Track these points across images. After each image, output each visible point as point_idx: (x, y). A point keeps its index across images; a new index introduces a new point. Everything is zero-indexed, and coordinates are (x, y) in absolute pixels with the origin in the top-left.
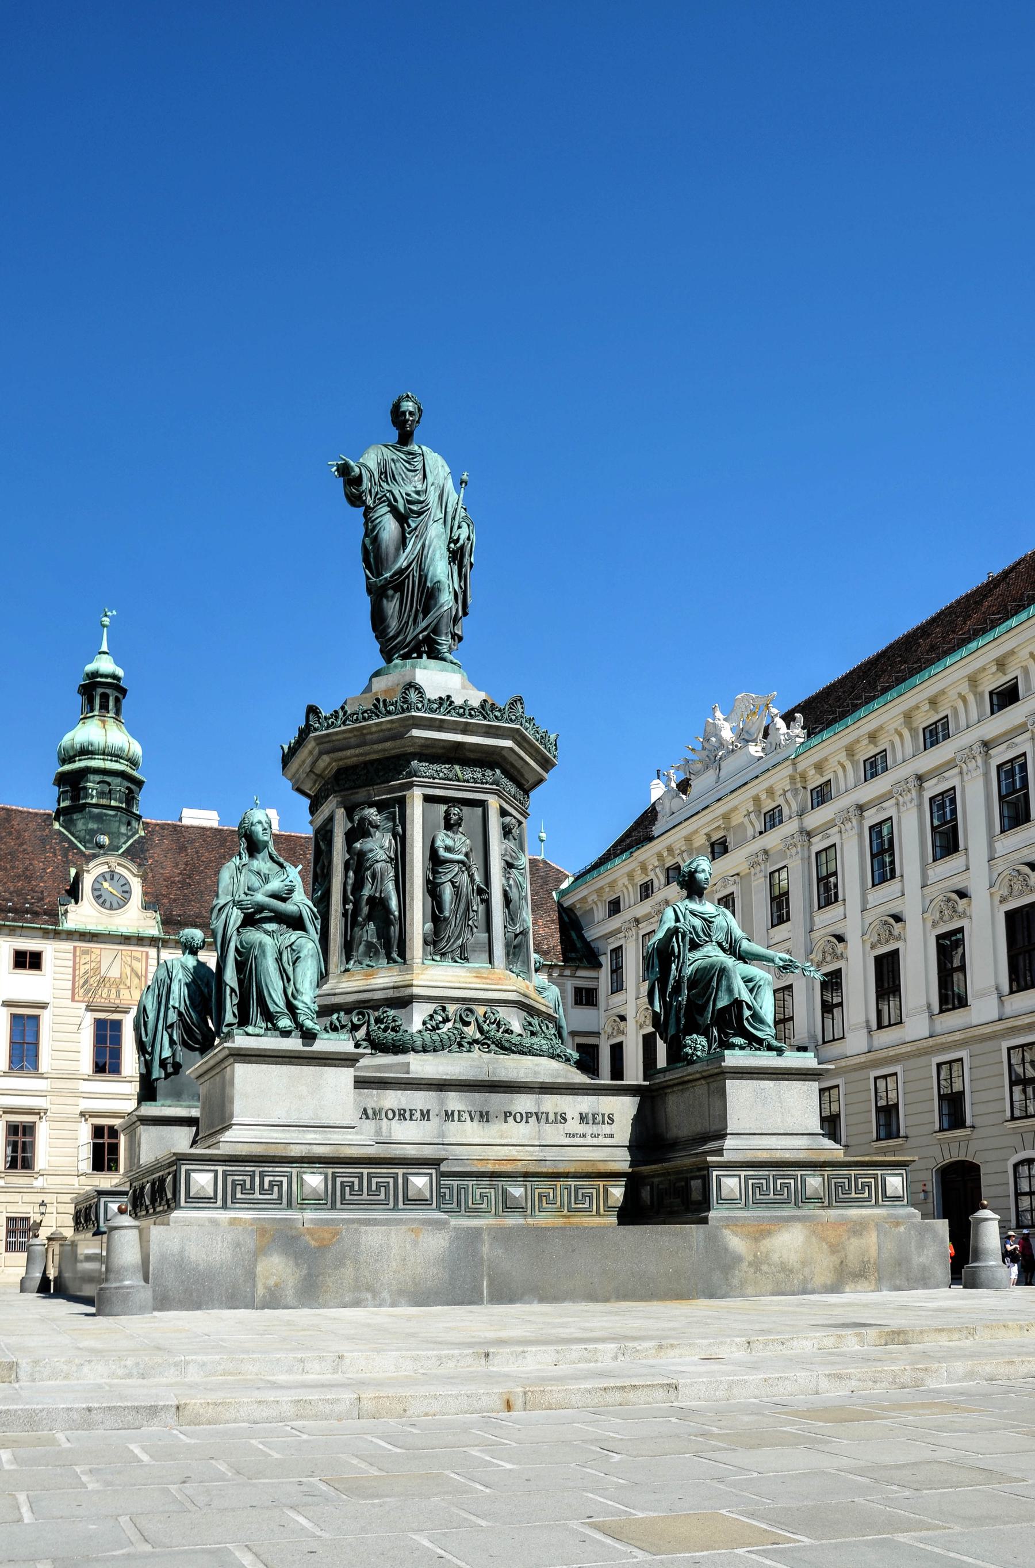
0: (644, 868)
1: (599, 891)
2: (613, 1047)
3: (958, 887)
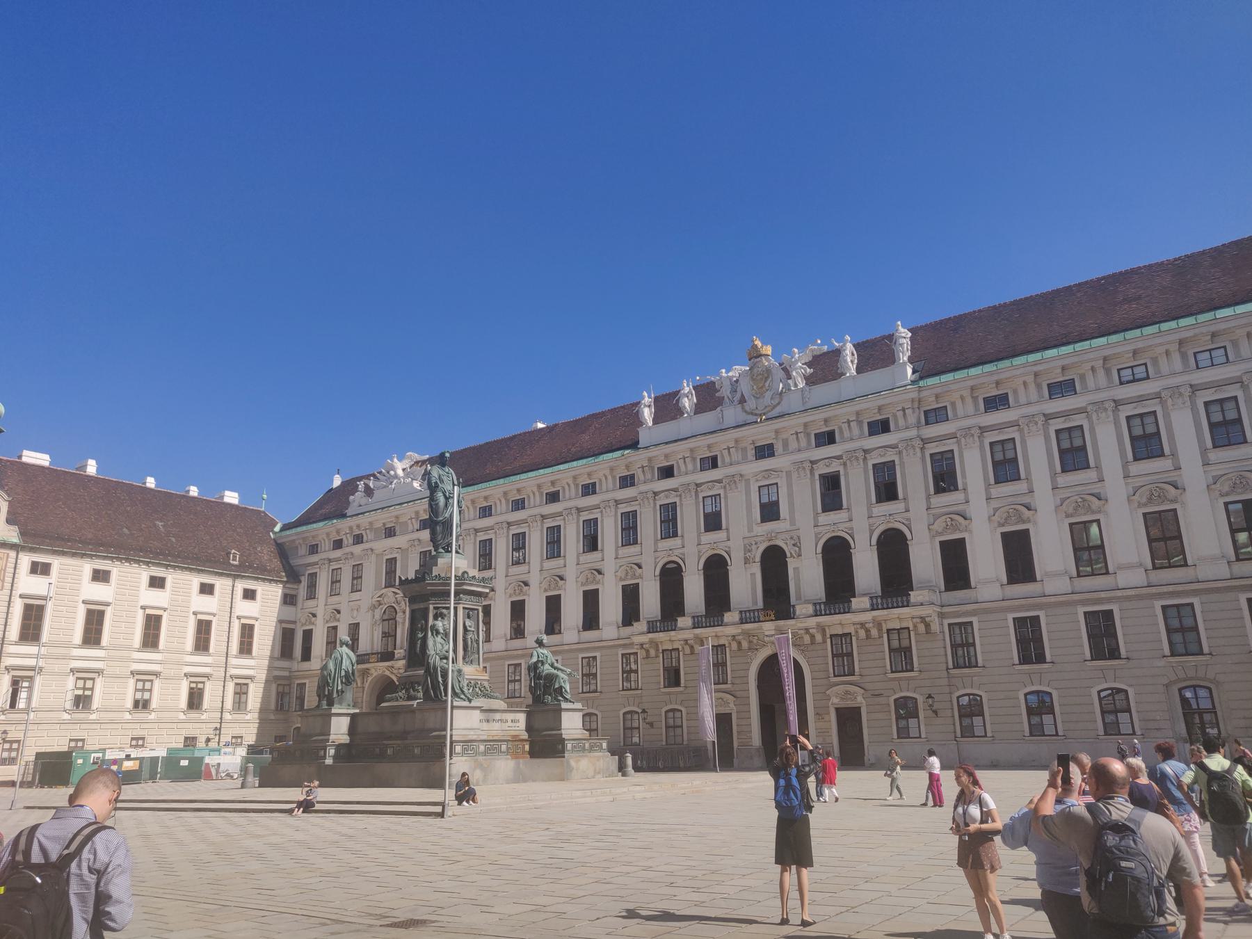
0: (338, 532)
1: (304, 539)
2: (304, 631)
3: (525, 580)
